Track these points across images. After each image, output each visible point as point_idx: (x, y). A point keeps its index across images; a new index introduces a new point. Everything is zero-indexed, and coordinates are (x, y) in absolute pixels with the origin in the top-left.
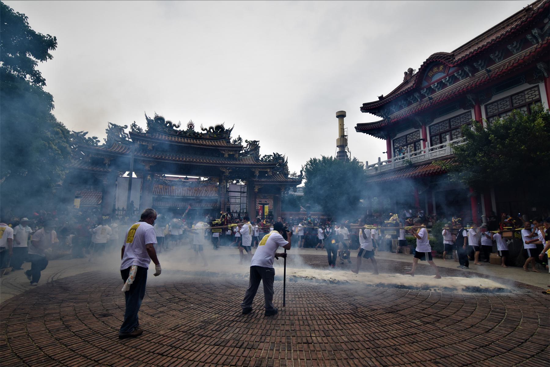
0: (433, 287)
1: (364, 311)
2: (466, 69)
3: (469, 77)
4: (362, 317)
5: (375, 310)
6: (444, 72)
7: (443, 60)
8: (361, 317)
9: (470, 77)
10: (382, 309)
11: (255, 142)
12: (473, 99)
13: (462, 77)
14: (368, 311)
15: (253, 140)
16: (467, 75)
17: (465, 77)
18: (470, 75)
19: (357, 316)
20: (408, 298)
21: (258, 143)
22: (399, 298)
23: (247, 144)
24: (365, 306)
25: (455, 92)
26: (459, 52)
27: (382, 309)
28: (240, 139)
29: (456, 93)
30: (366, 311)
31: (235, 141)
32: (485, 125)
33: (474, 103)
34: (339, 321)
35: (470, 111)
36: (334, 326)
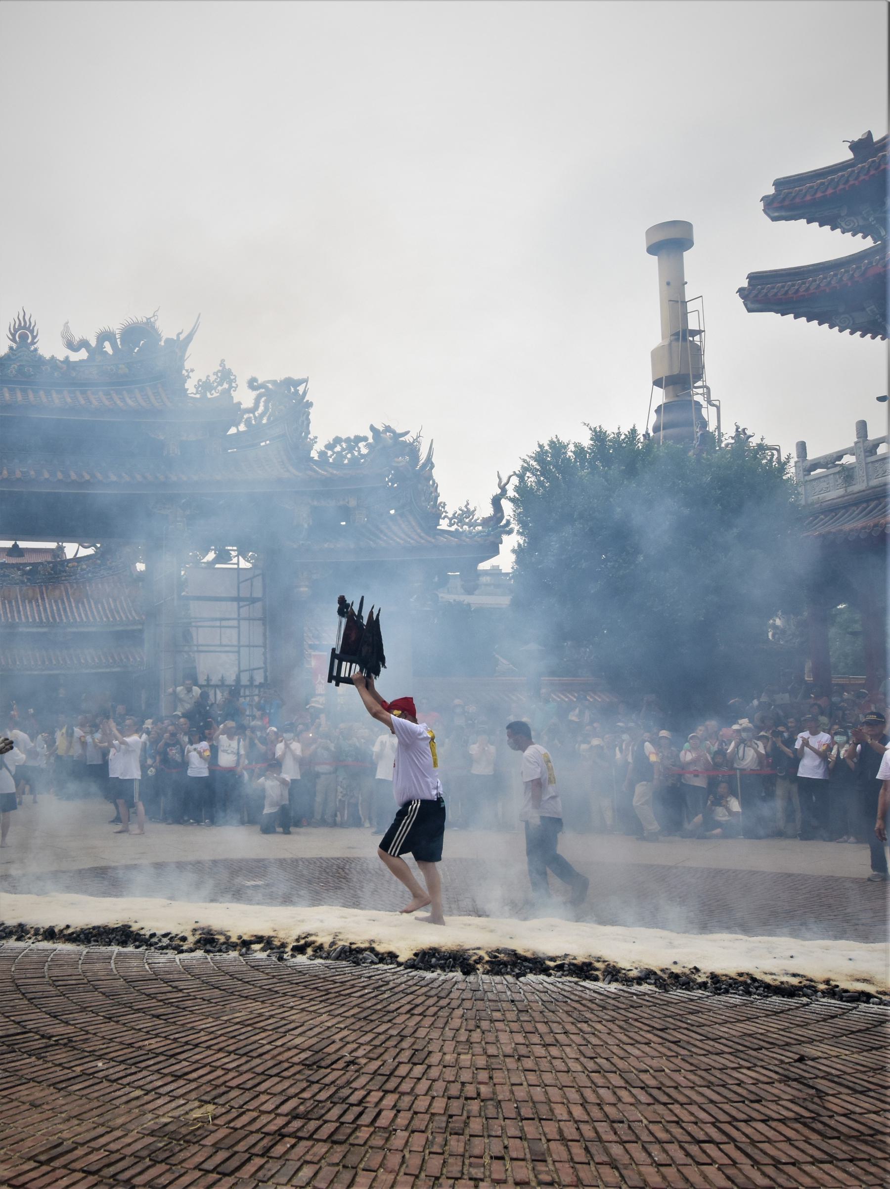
1: (858, 1110)
4: (857, 1138)
8: (850, 1137)
11: (290, 383)
14: (875, 1113)
15: (280, 377)
19: (830, 1133)
21: (301, 389)
23: (254, 394)
28: (226, 375)
30: (870, 1112)
31: (205, 386)
34: (750, 1150)
36: (731, 1171)
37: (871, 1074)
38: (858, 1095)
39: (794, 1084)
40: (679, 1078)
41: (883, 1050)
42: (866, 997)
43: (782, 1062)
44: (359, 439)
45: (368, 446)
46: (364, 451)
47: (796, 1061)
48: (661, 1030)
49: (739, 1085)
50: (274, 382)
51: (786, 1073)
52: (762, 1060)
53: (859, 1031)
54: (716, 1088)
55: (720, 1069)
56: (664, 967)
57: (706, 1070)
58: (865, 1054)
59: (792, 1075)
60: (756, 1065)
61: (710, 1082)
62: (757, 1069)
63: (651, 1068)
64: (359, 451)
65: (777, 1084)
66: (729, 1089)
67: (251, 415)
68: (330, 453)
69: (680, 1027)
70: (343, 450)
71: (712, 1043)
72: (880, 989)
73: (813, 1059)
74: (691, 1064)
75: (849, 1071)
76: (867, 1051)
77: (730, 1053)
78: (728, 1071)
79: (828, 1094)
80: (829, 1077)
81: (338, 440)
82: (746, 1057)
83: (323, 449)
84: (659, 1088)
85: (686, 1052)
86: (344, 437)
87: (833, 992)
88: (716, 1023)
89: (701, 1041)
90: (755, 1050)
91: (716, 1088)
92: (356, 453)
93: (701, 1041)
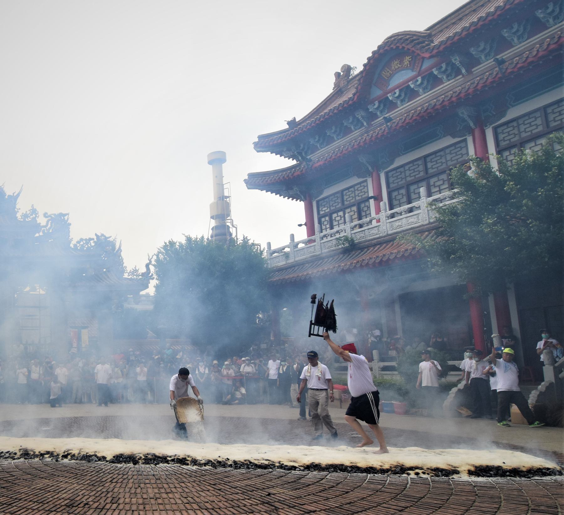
0: (411, 469)
2: (455, 60)
3: (461, 76)
5: (311, 511)
6: (413, 71)
7: (409, 47)
9: (463, 76)
10: (324, 510)
11: (62, 215)
12: (469, 116)
13: (448, 76)
15: (57, 212)
16: (458, 72)
17: (453, 75)
18: (464, 71)
20: (368, 489)
21: (66, 218)
22: (352, 491)
23: (46, 219)
24: (292, 506)
25: (435, 105)
26: (440, 29)
27: (324, 510)
28: (34, 211)
29: (437, 107)
31: (25, 216)
32: (494, 164)
33: (472, 124)
35: (465, 141)
37: (296, 499)
38: (291, 508)
39: (266, 505)
40: (221, 504)
41: (301, 489)
42: (294, 468)
43: (261, 496)
44: (91, 239)
45: (94, 242)
46: (93, 244)
47: (267, 495)
48: (214, 485)
49: (244, 506)
50: (55, 215)
51: (263, 500)
52: (254, 496)
53: (292, 482)
54: (235, 508)
55: (237, 500)
56: (215, 458)
57: (231, 501)
58: (294, 491)
59: (265, 501)
60: (251, 498)
61: (233, 506)
62: (252, 499)
63: (210, 501)
64: (91, 244)
65: (259, 505)
66: (241, 508)
67: (45, 228)
68: (78, 245)
69: (221, 483)
70: (84, 244)
71: (234, 489)
72: (300, 465)
73: (274, 494)
74: (226, 498)
75: (288, 498)
76: (295, 490)
77: (241, 493)
78: (241, 501)
79: (279, 509)
80: (280, 502)
81: (82, 240)
82: (247, 495)
83: (75, 243)
84: (213, 509)
85: (223, 494)
86: (84, 238)
87: (282, 466)
88: (236, 481)
89: (229, 489)
90: (251, 491)
91: (235, 508)
92: (89, 245)
93: (229, 489)
